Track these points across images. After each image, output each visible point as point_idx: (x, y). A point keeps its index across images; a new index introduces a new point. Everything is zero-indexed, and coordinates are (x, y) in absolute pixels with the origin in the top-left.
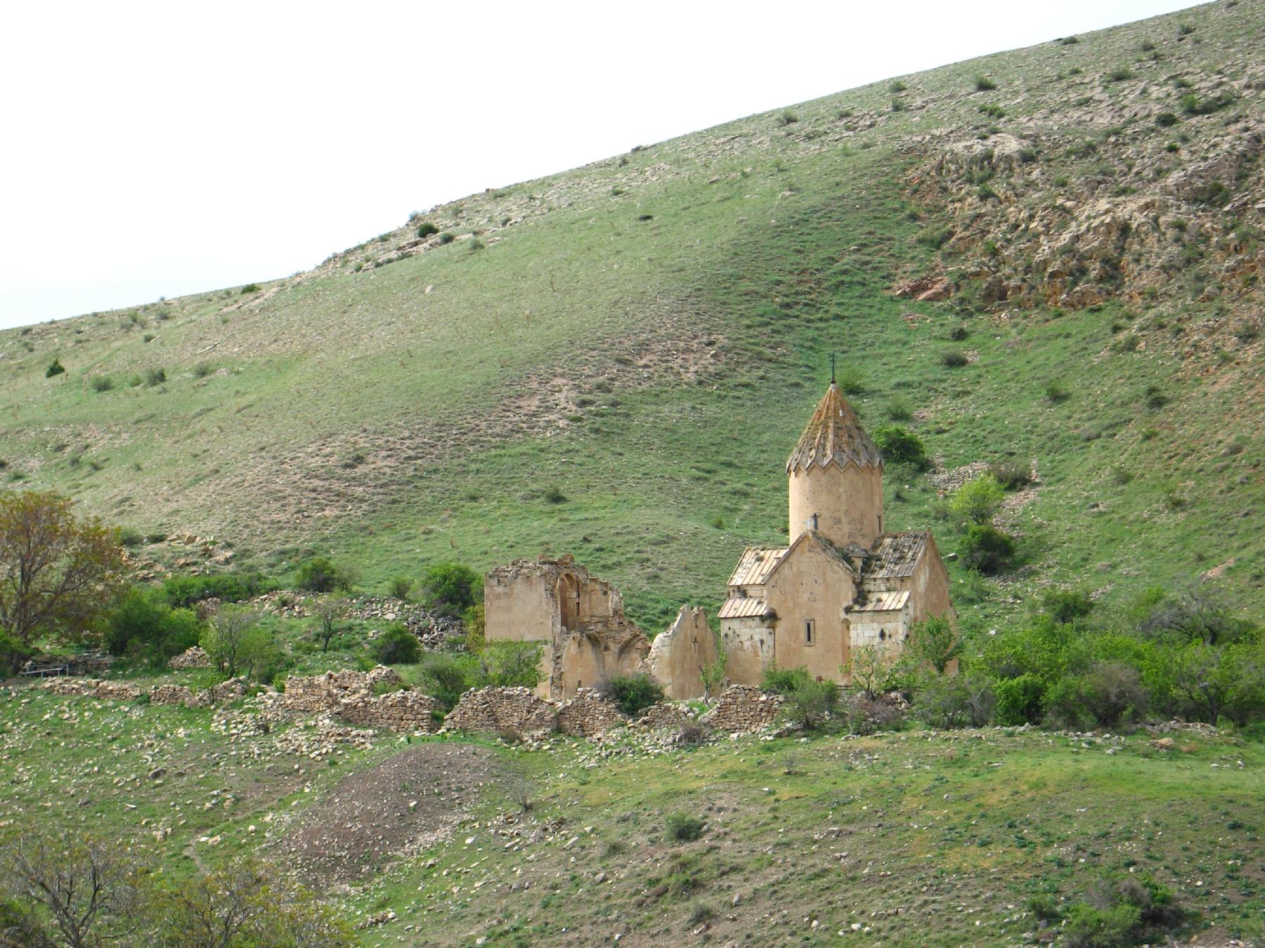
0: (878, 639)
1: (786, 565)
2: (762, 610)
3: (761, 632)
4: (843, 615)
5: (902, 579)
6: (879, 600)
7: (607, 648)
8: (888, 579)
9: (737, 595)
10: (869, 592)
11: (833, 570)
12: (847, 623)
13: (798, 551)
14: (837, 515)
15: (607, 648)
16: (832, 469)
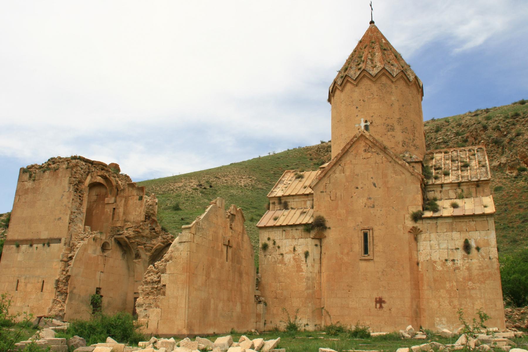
0: (460, 254)
1: (338, 168)
2: (307, 219)
3: (305, 243)
4: (410, 224)
5: (478, 184)
6: (455, 206)
7: (138, 256)
8: (459, 184)
9: (278, 206)
10: (435, 199)
11: (395, 172)
12: (415, 233)
13: (353, 152)
14: (389, 121)
15: (138, 256)
16: (384, 79)
